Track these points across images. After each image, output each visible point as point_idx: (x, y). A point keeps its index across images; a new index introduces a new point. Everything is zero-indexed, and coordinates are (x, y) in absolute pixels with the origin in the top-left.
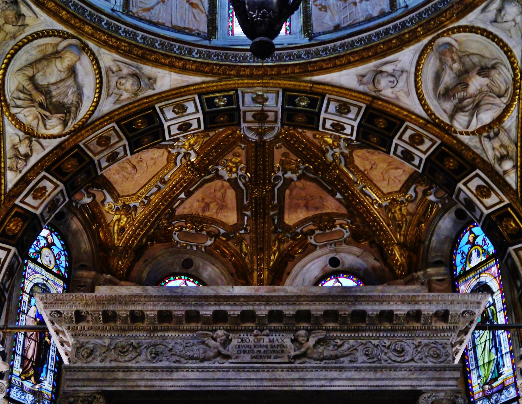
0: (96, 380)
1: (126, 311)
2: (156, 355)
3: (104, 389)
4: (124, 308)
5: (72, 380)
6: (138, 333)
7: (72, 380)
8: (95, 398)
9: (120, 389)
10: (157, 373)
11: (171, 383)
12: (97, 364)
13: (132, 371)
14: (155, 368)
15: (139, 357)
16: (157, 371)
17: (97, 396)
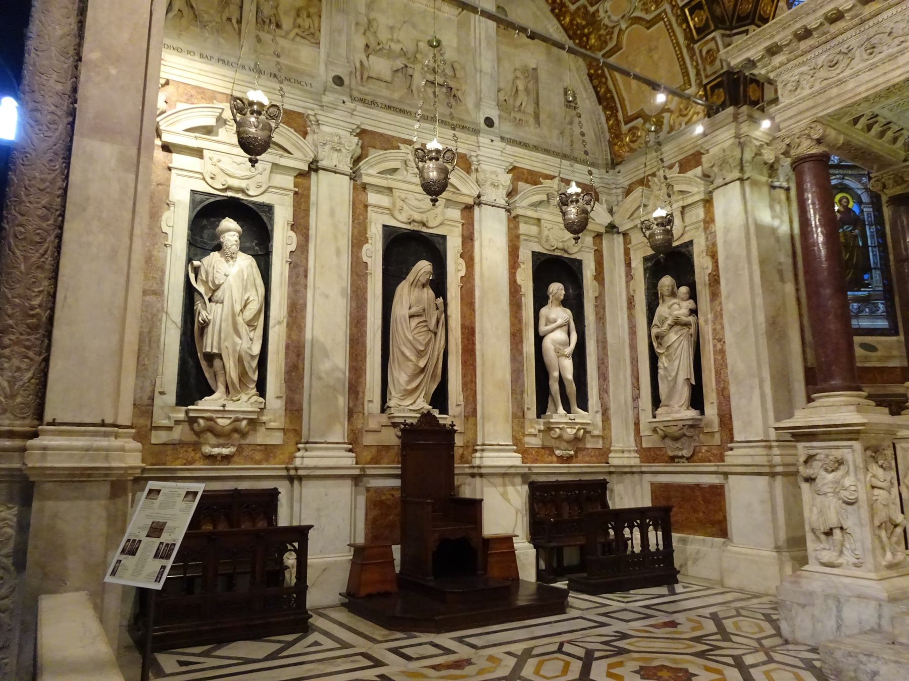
0: (808, 110)
1: (816, 19)
2: (872, 50)
3: (820, 114)
4: (811, 17)
5: (785, 120)
6: (844, 36)
7: (785, 120)
8: (811, 128)
9: (838, 106)
10: (877, 69)
11: (898, 72)
12: (807, 92)
13: (846, 81)
14: (872, 65)
15: (853, 61)
16: (877, 66)
17: (813, 125)
